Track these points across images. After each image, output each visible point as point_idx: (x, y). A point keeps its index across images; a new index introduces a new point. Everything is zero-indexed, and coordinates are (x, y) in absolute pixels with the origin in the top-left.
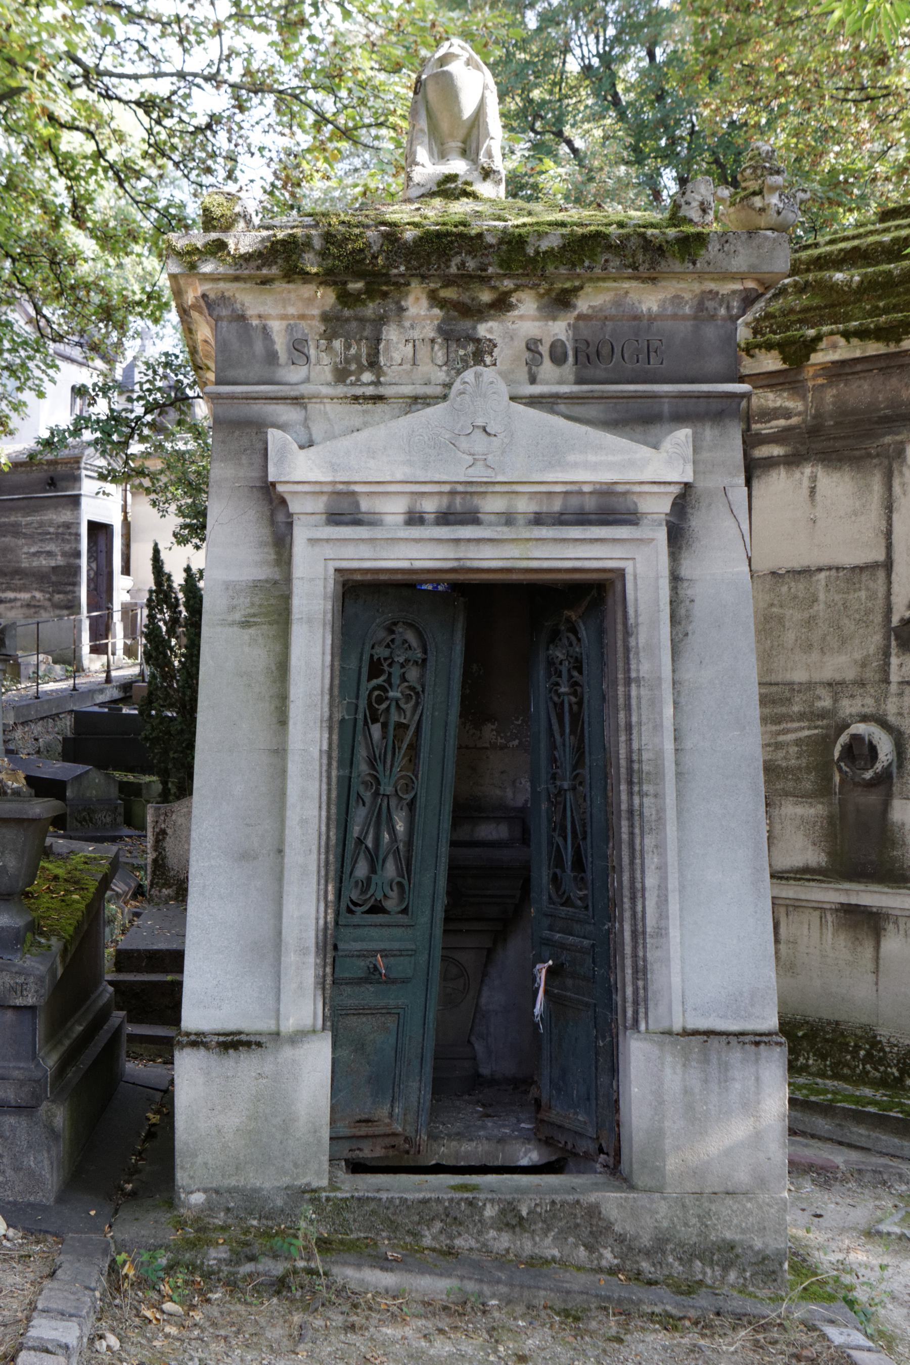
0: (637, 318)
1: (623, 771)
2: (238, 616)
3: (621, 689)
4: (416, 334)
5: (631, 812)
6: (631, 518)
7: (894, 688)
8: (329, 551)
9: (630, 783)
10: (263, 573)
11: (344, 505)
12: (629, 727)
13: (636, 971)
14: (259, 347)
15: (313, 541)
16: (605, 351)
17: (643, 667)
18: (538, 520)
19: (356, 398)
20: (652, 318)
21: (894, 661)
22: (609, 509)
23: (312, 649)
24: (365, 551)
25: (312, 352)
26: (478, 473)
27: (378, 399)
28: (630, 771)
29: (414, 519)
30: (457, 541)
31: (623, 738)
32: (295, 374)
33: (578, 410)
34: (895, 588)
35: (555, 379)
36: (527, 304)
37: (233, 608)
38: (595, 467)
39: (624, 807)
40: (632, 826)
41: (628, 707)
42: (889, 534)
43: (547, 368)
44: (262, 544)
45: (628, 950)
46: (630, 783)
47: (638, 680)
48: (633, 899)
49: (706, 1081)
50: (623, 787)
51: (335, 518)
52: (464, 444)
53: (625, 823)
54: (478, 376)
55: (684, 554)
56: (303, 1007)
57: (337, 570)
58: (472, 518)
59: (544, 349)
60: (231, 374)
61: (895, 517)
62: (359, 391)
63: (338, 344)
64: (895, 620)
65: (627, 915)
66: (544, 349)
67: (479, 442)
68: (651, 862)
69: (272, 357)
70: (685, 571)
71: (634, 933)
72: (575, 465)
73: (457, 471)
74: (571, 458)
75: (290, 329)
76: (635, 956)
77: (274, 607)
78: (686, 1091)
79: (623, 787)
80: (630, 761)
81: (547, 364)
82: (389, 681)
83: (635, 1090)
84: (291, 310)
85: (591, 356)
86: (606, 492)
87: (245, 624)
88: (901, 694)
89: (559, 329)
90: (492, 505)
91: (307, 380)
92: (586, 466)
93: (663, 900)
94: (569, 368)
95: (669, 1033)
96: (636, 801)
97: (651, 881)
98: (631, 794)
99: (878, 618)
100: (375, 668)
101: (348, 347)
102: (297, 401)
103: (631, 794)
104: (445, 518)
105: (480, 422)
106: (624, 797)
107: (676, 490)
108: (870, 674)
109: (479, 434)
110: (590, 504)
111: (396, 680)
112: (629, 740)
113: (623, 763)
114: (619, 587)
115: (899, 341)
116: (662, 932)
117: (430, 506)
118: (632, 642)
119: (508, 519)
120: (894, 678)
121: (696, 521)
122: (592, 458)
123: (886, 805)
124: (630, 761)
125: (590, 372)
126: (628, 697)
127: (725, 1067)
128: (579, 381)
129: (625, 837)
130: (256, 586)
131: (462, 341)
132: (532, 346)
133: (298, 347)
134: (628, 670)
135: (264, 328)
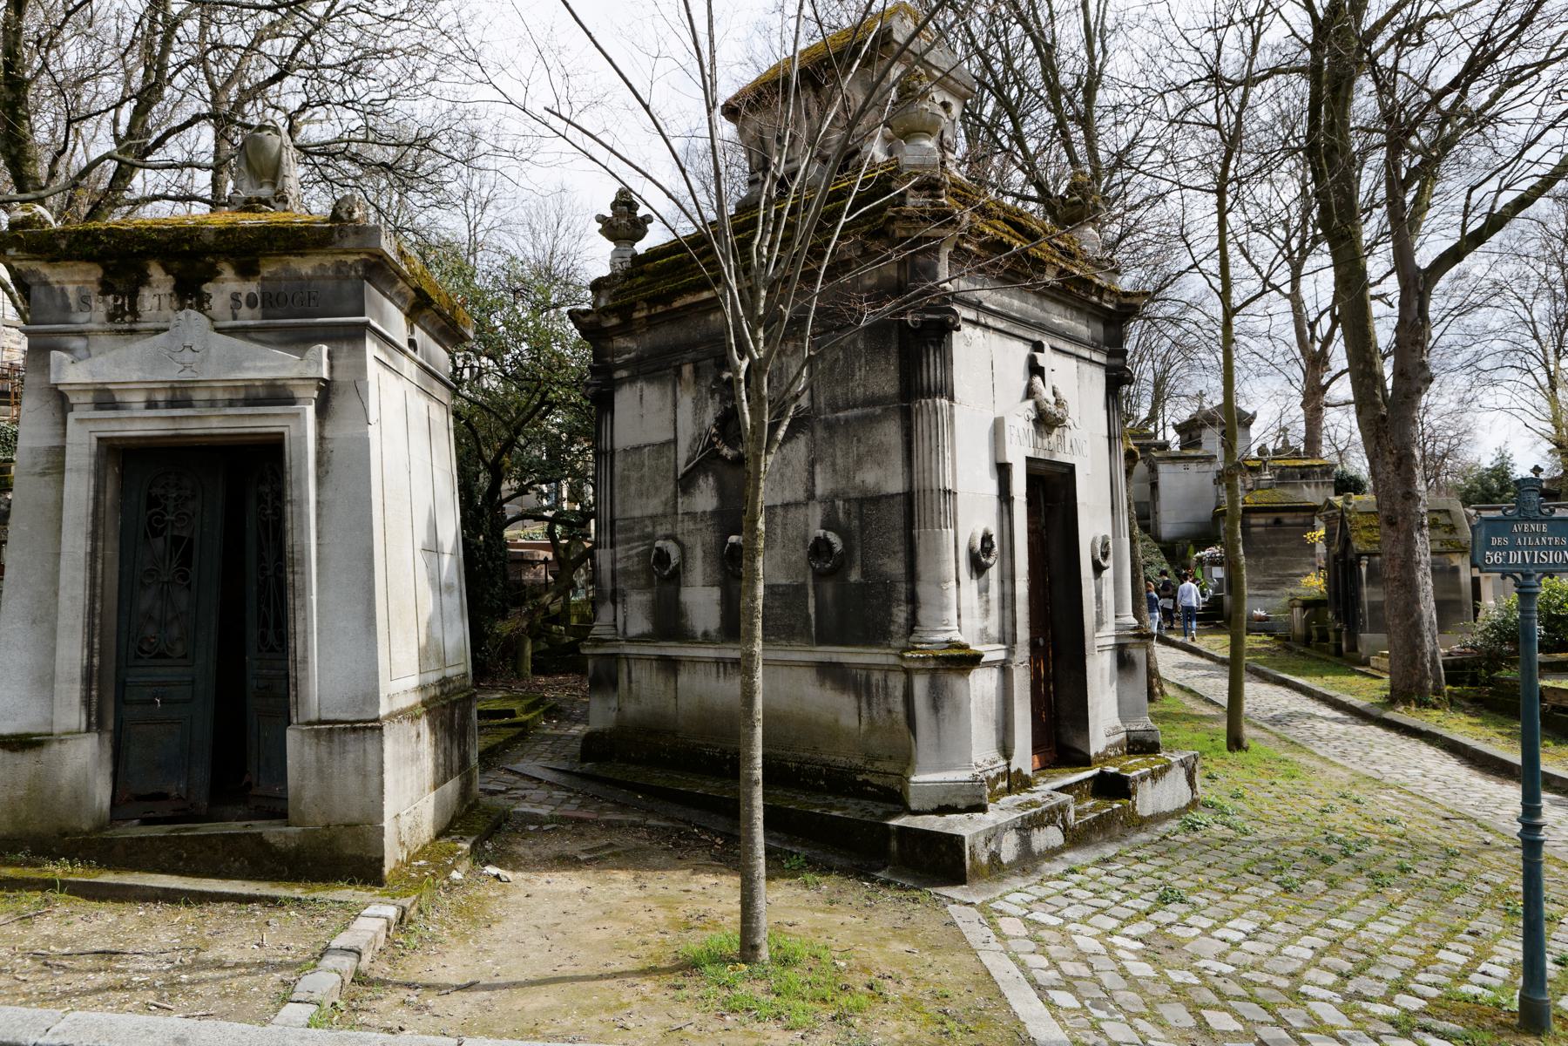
0: (300, 278)
2: (38, 469)
4: (160, 291)
6: (291, 401)
11: (105, 398)
14: (59, 301)
16: (281, 298)
18: (231, 403)
19: (119, 332)
20: (310, 279)
22: (277, 395)
23: (78, 489)
24: (116, 426)
26: (187, 375)
27: (132, 332)
29: (151, 404)
30: (173, 418)
32: (81, 317)
33: (262, 336)
35: (248, 317)
36: (228, 272)
37: (34, 464)
38: (261, 369)
43: (244, 310)
49: (330, 753)
51: (99, 406)
52: (177, 357)
54: (188, 315)
56: (71, 715)
57: (99, 439)
58: (188, 403)
59: (243, 299)
60: (40, 318)
62: (119, 327)
63: (110, 298)
66: (243, 299)
67: (188, 354)
69: (67, 307)
70: (327, 434)
72: (248, 369)
73: (173, 374)
74: (246, 364)
75: (79, 290)
77: (56, 461)
78: (319, 760)
81: (244, 306)
82: (165, 509)
84: (77, 278)
85: (270, 302)
86: (271, 384)
87: (43, 474)
89: (252, 287)
90: (200, 395)
91: (90, 321)
92: (255, 369)
94: (257, 311)
95: (309, 723)
97: (299, 628)
99: (672, 475)
100: (152, 502)
101: (116, 300)
102: (81, 334)
104: (172, 404)
108: (669, 510)
110: (262, 393)
111: (171, 509)
117: (160, 397)
119: (212, 403)
121: (335, 403)
122: (259, 364)
123: (678, 592)
125: (272, 312)
127: (344, 744)
131: (189, 292)
132: (235, 297)
133: (84, 301)
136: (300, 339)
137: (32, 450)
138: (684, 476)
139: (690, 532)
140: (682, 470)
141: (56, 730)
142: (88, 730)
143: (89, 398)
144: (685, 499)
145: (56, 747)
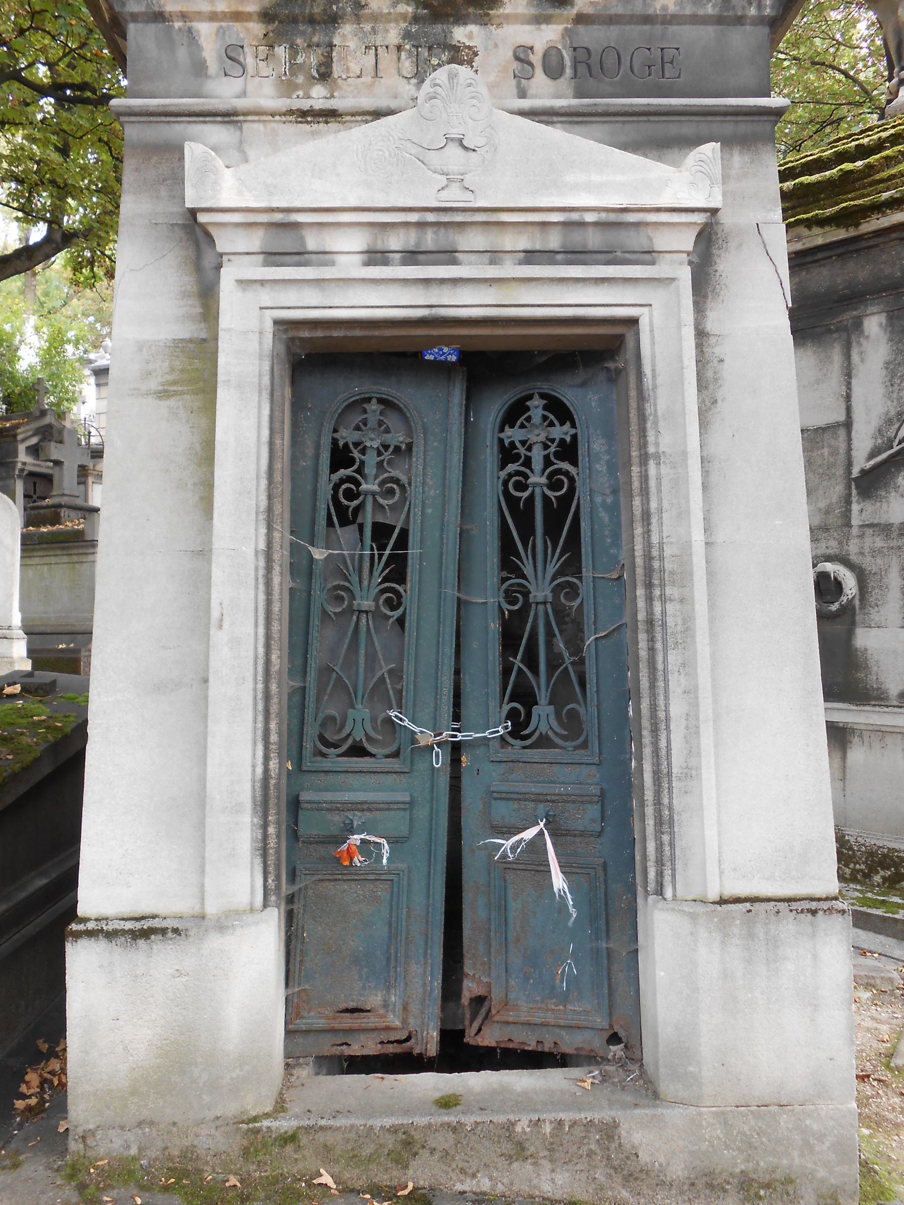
1: (640, 571)
2: (154, 384)
3: (635, 470)
5: (650, 622)
7: (855, 531)
8: (266, 297)
9: (649, 586)
10: (185, 331)
11: (286, 243)
12: (646, 516)
13: (659, 821)
15: (244, 284)
16: (610, 60)
17: (662, 439)
21: (855, 507)
23: (245, 417)
24: (311, 297)
25: (250, 61)
28: (649, 571)
30: (427, 282)
31: (639, 531)
34: (855, 443)
39: (641, 616)
40: (652, 640)
41: (645, 492)
42: (848, 398)
44: (185, 295)
45: (649, 795)
46: (649, 586)
47: (657, 456)
48: (655, 731)
50: (640, 592)
52: (434, 158)
53: (642, 637)
54: (452, 76)
55: (710, 304)
57: (277, 322)
59: (536, 59)
61: (854, 382)
63: (281, 51)
64: (855, 472)
65: (647, 751)
66: (536, 59)
68: (677, 683)
69: (199, 68)
70: (710, 326)
71: (657, 774)
73: (427, 193)
74: (570, 178)
76: (658, 802)
77: (194, 371)
79: (640, 592)
80: (648, 558)
81: (539, 75)
83: (661, 974)
87: (163, 394)
88: (861, 536)
91: (244, 94)
92: (589, 187)
93: (693, 731)
94: (565, 83)
96: (657, 608)
97: (677, 708)
98: (649, 599)
99: (840, 471)
100: (341, 457)
103: (649, 599)
105: (455, 133)
106: (641, 604)
107: (700, 219)
108: (834, 520)
109: (453, 150)
112: (647, 533)
113: (639, 561)
114: (630, 343)
115: (857, 225)
116: (691, 773)
118: (649, 409)
120: (855, 521)
121: (726, 265)
122: (596, 178)
123: (850, 634)
124: (648, 558)
126: (644, 478)
128: (579, 94)
129: (643, 654)
130: (179, 346)
132: (522, 55)
133: (232, 55)
134: (643, 445)
135: (190, 30)
136: (660, 136)
137: (141, 346)
138: (864, 472)
139: (874, 552)
140: (861, 463)
141: (212, 908)
142: (265, 905)
143: (255, 241)
144: (869, 506)
145: (214, 942)
